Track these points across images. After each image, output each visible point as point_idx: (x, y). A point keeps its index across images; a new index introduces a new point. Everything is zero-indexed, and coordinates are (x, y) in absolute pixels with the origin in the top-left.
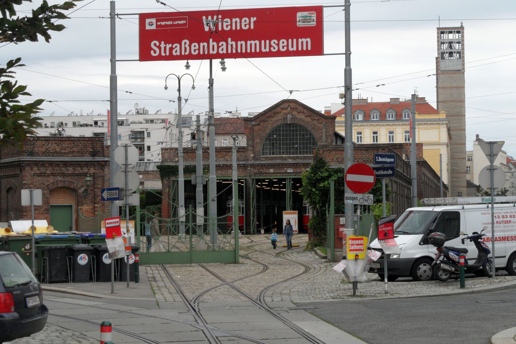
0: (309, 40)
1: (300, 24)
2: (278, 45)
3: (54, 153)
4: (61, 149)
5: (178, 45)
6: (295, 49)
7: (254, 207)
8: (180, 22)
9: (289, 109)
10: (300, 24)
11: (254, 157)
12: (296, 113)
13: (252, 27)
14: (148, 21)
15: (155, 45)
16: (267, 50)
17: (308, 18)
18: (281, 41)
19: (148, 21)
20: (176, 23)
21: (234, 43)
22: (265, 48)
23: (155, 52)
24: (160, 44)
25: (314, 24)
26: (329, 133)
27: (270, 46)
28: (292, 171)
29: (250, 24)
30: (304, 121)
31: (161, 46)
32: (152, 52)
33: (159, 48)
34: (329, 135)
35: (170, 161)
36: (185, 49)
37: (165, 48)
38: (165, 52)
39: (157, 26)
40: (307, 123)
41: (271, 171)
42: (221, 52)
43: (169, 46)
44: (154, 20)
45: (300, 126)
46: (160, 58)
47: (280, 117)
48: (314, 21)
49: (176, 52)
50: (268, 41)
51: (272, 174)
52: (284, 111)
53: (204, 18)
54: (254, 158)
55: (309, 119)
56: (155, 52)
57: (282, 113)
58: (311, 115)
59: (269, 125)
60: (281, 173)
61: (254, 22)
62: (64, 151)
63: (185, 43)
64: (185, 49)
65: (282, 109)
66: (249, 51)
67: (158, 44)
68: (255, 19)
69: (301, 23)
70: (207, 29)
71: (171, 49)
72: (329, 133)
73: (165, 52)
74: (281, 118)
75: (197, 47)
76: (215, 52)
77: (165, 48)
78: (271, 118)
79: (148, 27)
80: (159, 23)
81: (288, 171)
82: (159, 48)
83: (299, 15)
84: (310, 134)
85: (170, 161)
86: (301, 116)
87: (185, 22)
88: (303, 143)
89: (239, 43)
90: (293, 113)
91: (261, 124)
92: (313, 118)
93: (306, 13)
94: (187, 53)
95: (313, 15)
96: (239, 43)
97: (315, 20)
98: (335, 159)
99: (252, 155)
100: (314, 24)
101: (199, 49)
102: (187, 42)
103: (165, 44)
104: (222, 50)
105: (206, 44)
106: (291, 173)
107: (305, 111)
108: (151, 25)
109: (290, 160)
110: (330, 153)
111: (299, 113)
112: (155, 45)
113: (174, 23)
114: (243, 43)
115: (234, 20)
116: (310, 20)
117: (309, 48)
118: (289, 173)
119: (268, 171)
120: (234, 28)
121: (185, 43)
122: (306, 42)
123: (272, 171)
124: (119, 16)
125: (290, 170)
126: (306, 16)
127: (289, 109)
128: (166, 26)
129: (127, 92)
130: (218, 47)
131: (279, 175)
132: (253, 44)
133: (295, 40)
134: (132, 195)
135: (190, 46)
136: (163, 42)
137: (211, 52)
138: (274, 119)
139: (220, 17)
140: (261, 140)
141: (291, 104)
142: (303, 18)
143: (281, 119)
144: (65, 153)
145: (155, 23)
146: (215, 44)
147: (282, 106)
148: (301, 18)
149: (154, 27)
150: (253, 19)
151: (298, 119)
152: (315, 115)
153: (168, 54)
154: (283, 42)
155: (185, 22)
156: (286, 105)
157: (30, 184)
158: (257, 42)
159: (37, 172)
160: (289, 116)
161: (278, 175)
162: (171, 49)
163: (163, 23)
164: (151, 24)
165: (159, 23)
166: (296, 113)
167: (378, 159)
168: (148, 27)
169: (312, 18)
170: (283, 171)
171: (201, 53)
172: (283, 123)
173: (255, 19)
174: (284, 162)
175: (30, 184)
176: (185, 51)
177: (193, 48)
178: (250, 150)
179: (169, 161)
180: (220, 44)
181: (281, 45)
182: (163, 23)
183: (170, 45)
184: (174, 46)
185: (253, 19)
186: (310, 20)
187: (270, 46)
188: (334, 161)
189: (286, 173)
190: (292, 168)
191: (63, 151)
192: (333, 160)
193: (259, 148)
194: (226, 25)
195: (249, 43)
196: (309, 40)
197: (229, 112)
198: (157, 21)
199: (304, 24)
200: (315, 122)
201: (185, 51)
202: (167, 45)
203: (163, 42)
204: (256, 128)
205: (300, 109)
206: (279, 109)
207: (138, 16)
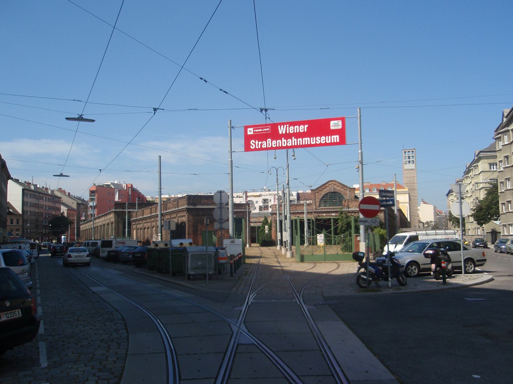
0: (338, 136)
1: (332, 128)
2: (320, 140)
3: (204, 204)
4: (208, 202)
5: (265, 142)
6: (330, 142)
8: (265, 130)
10: (332, 128)
12: (336, 187)
13: (306, 131)
14: (249, 129)
15: (253, 142)
16: (314, 143)
17: (337, 124)
18: (322, 137)
19: (249, 129)
20: (264, 130)
21: (296, 140)
22: (313, 142)
23: (253, 146)
24: (255, 142)
25: (340, 127)
27: (316, 141)
28: (334, 215)
29: (304, 129)
30: (340, 190)
31: (256, 143)
32: (251, 146)
33: (255, 144)
36: (269, 144)
37: (258, 144)
38: (258, 146)
39: (254, 132)
42: (288, 145)
43: (260, 143)
44: (252, 129)
45: (338, 193)
46: (255, 149)
47: (328, 188)
48: (340, 125)
49: (264, 146)
50: (314, 138)
51: (324, 216)
52: (330, 186)
53: (279, 126)
54: (316, 209)
55: (342, 189)
56: (253, 146)
61: (307, 127)
62: (210, 203)
63: (269, 141)
64: (269, 144)
66: (304, 144)
67: (254, 142)
68: (307, 126)
69: (333, 127)
70: (280, 133)
71: (261, 144)
73: (258, 146)
75: (275, 143)
76: (285, 145)
77: (258, 144)
78: (324, 189)
79: (249, 133)
80: (254, 131)
81: (332, 215)
82: (255, 144)
83: (332, 123)
84: (343, 197)
86: (339, 188)
87: (268, 129)
88: (340, 201)
89: (299, 140)
90: (334, 187)
91: (319, 192)
93: (336, 122)
94: (270, 146)
95: (339, 123)
96: (299, 140)
97: (341, 125)
98: (354, 206)
100: (340, 127)
101: (277, 144)
102: (270, 140)
103: (258, 142)
104: (289, 144)
105: (280, 141)
107: (340, 185)
108: (250, 131)
110: (352, 202)
112: (253, 142)
113: (263, 130)
114: (301, 139)
115: (295, 127)
116: (338, 125)
117: (338, 141)
119: (322, 215)
120: (295, 132)
121: (269, 141)
122: (336, 138)
123: (324, 215)
124: (233, 128)
125: (333, 214)
126: (336, 123)
128: (259, 132)
129: (236, 167)
130: (287, 142)
132: (306, 140)
133: (330, 137)
134: (224, 223)
135: (272, 142)
136: (257, 141)
137: (283, 145)
138: (325, 190)
139: (288, 126)
142: (334, 125)
143: (328, 190)
144: (210, 204)
145: (252, 131)
146: (285, 141)
147: (329, 183)
148: (333, 125)
149: (252, 133)
150: (306, 126)
151: (337, 189)
152: (345, 187)
153: (260, 147)
154: (323, 138)
155: (268, 129)
156: (331, 183)
157: (191, 220)
158: (309, 139)
159: (195, 214)
160: (332, 188)
162: (261, 144)
163: (257, 131)
164: (250, 131)
165: (254, 131)
167: (382, 194)
168: (249, 133)
169: (339, 124)
170: (330, 215)
171: (278, 146)
172: (330, 191)
173: (307, 126)
175: (191, 220)
176: (269, 145)
177: (273, 144)
178: (314, 205)
180: (288, 141)
181: (322, 140)
182: (257, 131)
183: (261, 142)
184: (263, 143)
185: (306, 126)
186: (338, 125)
187: (316, 141)
188: (354, 207)
191: (209, 203)
192: (353, 206)
193: (318, 204)
194: (291, 130)
195: (304, 139)
196: (338, 136)
197: (296, 179)
198: (254, 129)
199: (335, 127)
201: (269, 145)
202: (259, 142)
203: (257, 141)
204: (316, 194)
205: (338, 184)
206: (327, 185)
207: (243, 127)
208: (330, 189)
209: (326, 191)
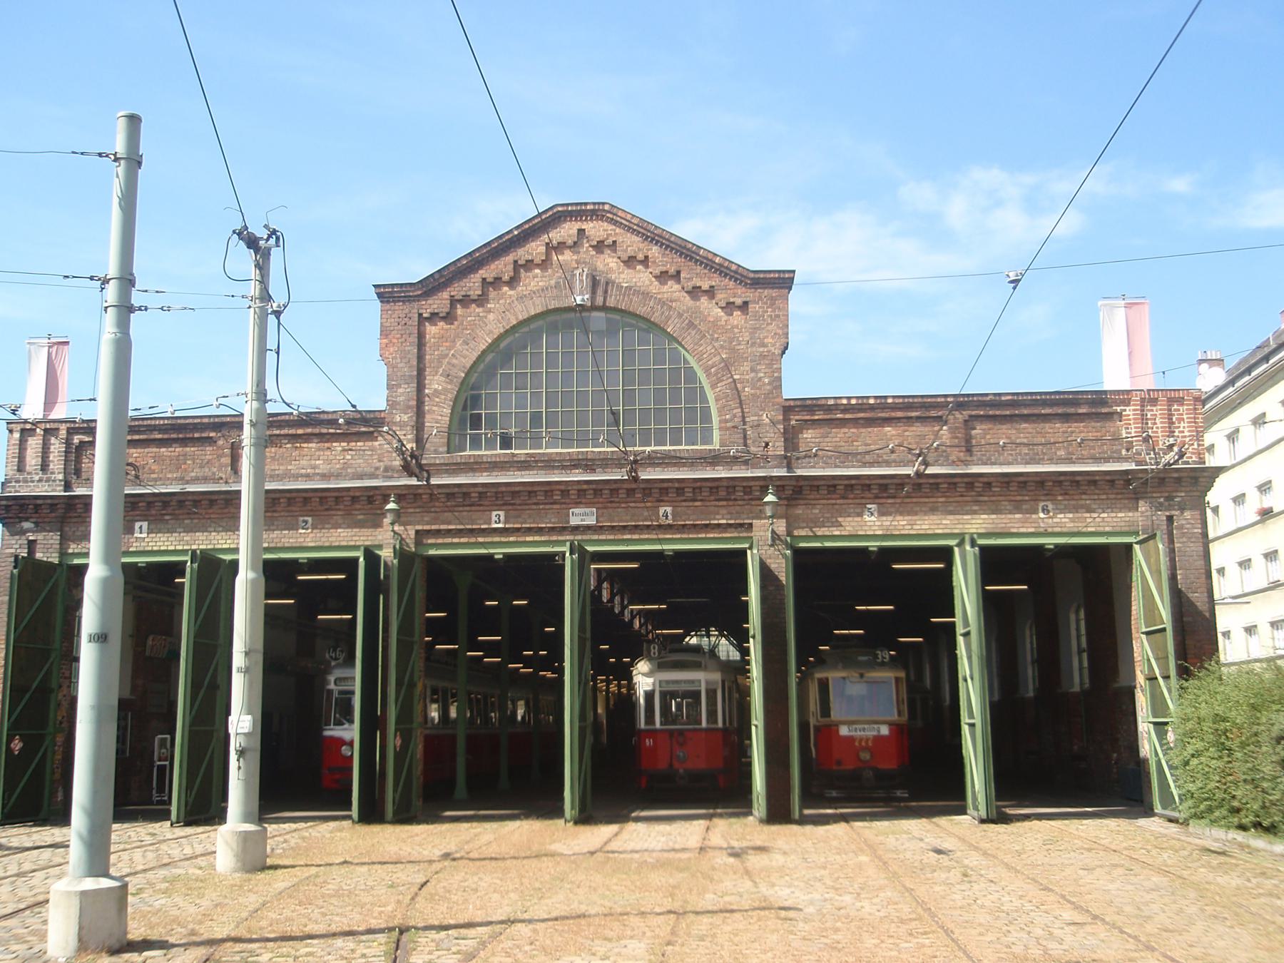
7: (412, 685)
26: (764, 345)
28: (591, 521)
30: (646, 295)
34: (763, 356)
35: (40, 480)
40: (662, 303)
41: (494, 518)
58: (679, 272)
59: (491, 316)
72: (764, 345)
81: (574, 521)
85: (40, 480)
92: (690, 285)
106: (588, 528)
107: (654, 251)
118: (576, 529)
123: (497, 519)
125: (581, 516)
140: (451, 382)
141: (589, 226)
151: (620, 287)
156: (567, 231)
161: (529, 539)
166: (611, 265)
179: (37, 478)
189: (564, 529)
190: (589, 504)
205: (631, 244)
206: (536, 249)
208: (557, 286)
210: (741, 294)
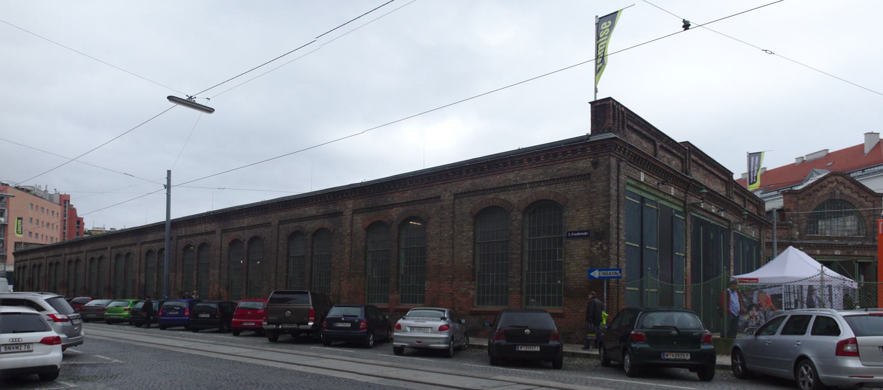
9: (836, 183)
11: (800, 235)
12: (843, 188)
28: (839, 253)
30: (850, 197)
47: (825, 191)
52: (831, 185)
54: (800, 237)
57: (828, 188)
60: (826, 255)
65: (829, 183)
74: (826, 192)
81: (836, 253)
86: (847, 192)
99: (797, 233)
107: (853, 186)
109: (837, 241)
111: (845, 188)
125: (837, 252)
127: (836, 183)
131: (825, 257)
138: (819, 194)
143: (827, 194)
151: (844, 194)
170: (831, 253)
172: (830, 198)
174: (831, 242)
178: (796, 227)
190: (840, 250)
200: (862, 200)
204: (801, 202)
209: (822, 196)
210: (873, 199)
